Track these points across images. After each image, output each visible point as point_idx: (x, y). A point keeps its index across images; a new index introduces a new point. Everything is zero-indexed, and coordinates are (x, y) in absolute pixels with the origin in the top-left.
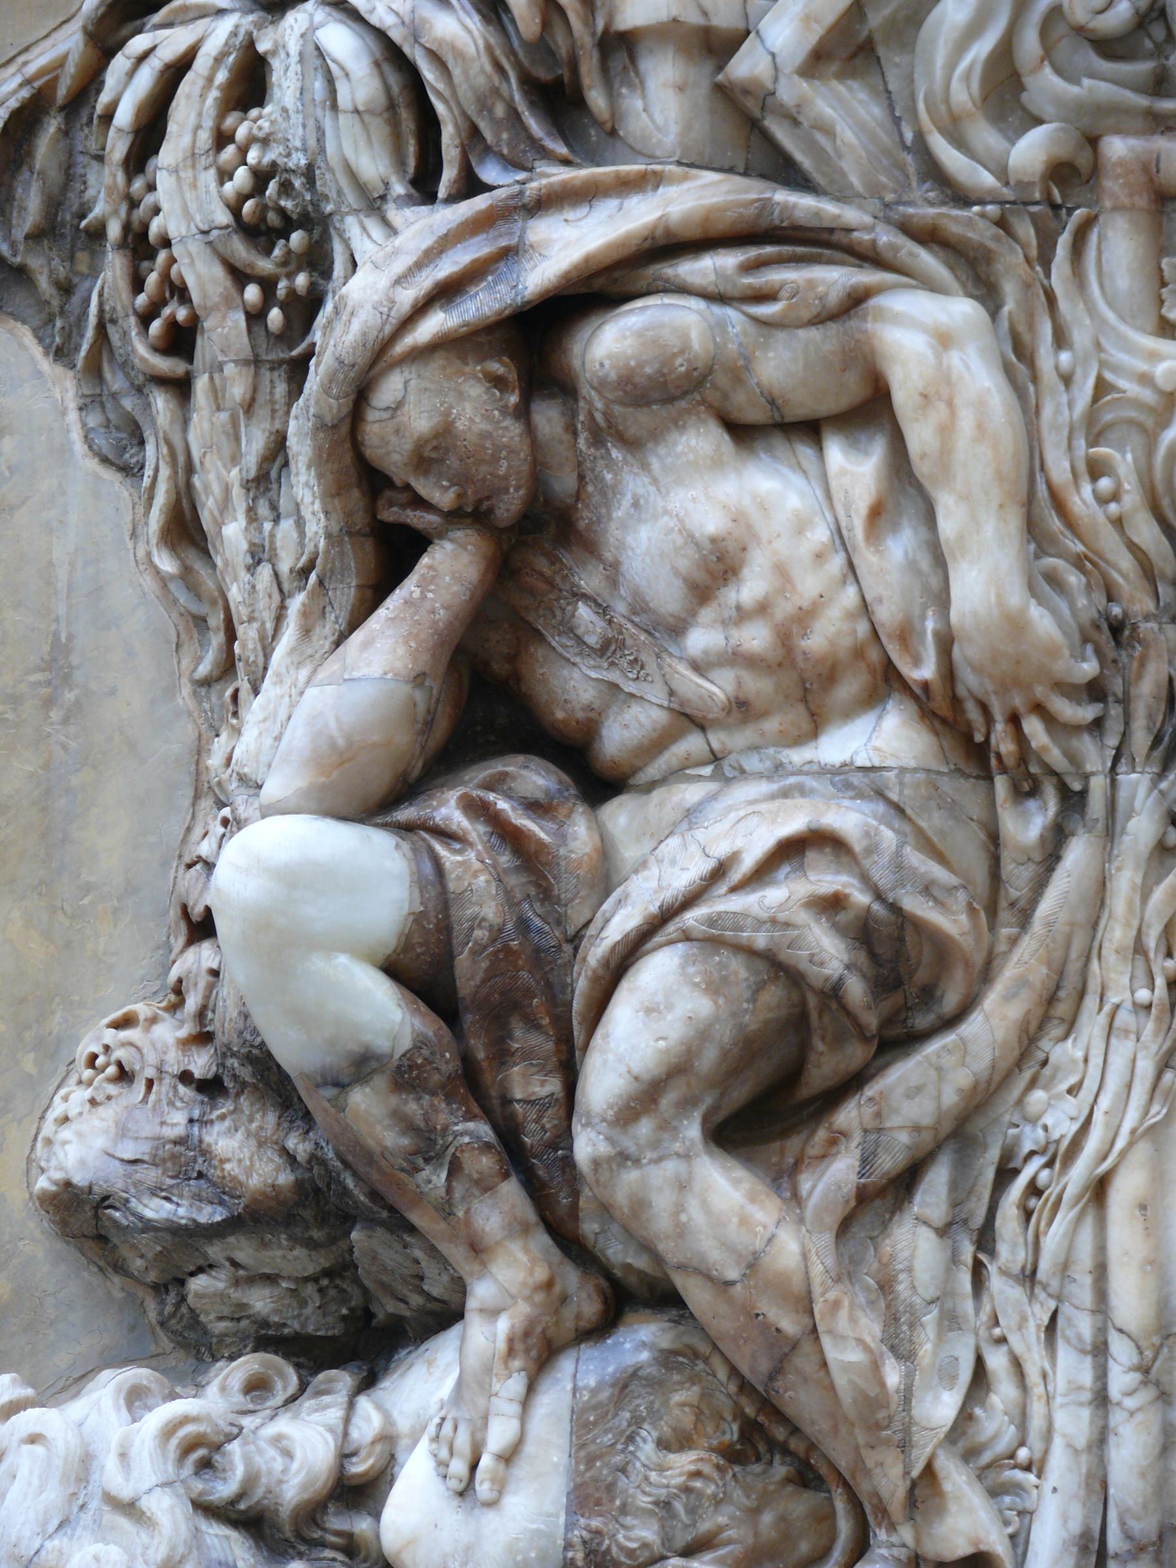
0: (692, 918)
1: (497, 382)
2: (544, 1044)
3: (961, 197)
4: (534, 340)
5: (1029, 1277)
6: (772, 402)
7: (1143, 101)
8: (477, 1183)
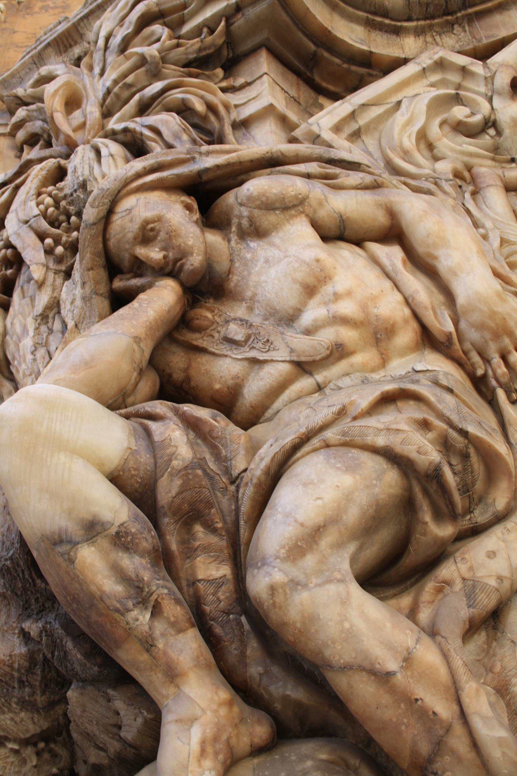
0: (330, 434)
1: (188, 207)
2: (219, 542)
3: (413, 177)
6: (341, 216)
7: (491, 155)
8: (173, 625)
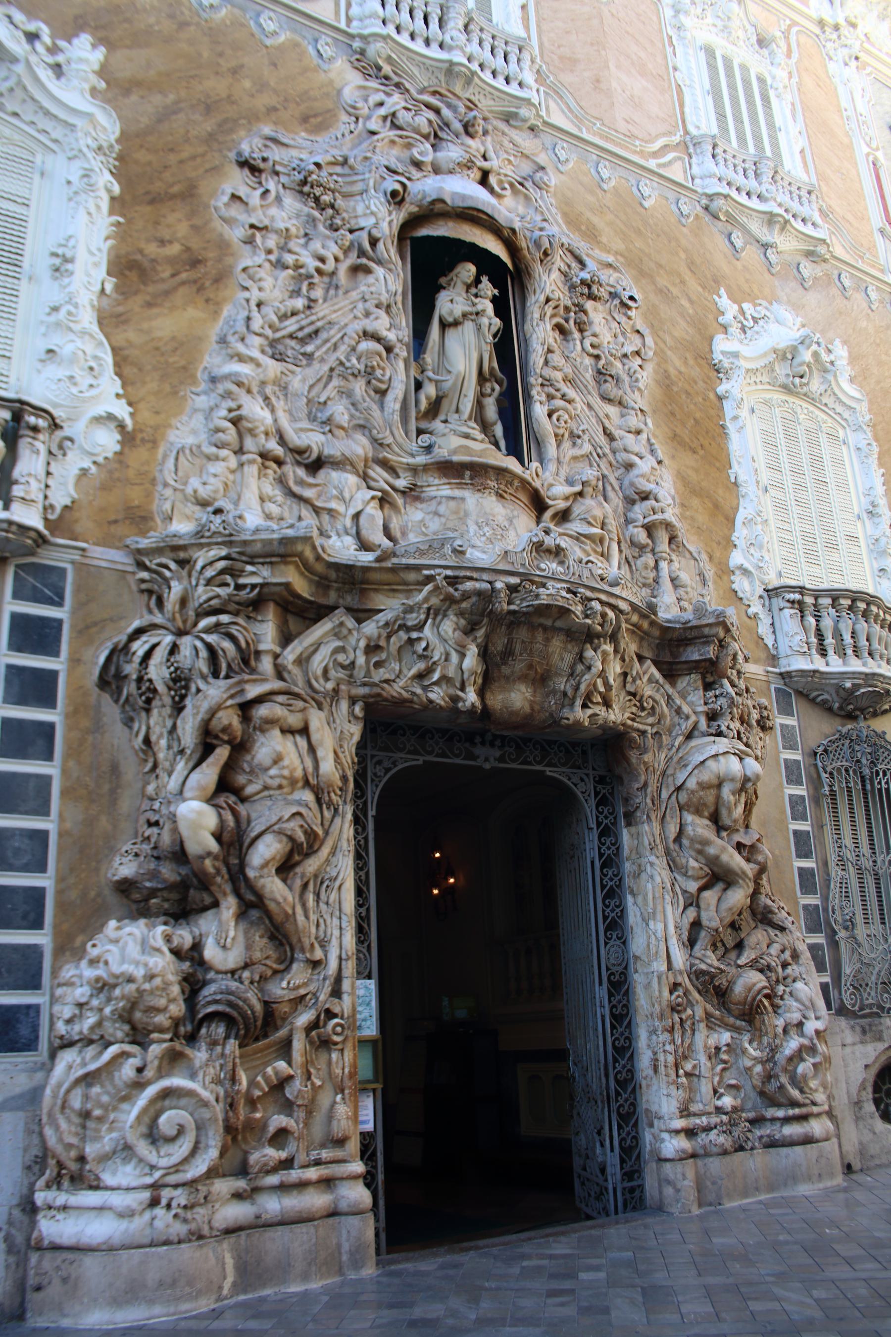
0: (276, 828)
4: (246, 708)
5: (327, 903)
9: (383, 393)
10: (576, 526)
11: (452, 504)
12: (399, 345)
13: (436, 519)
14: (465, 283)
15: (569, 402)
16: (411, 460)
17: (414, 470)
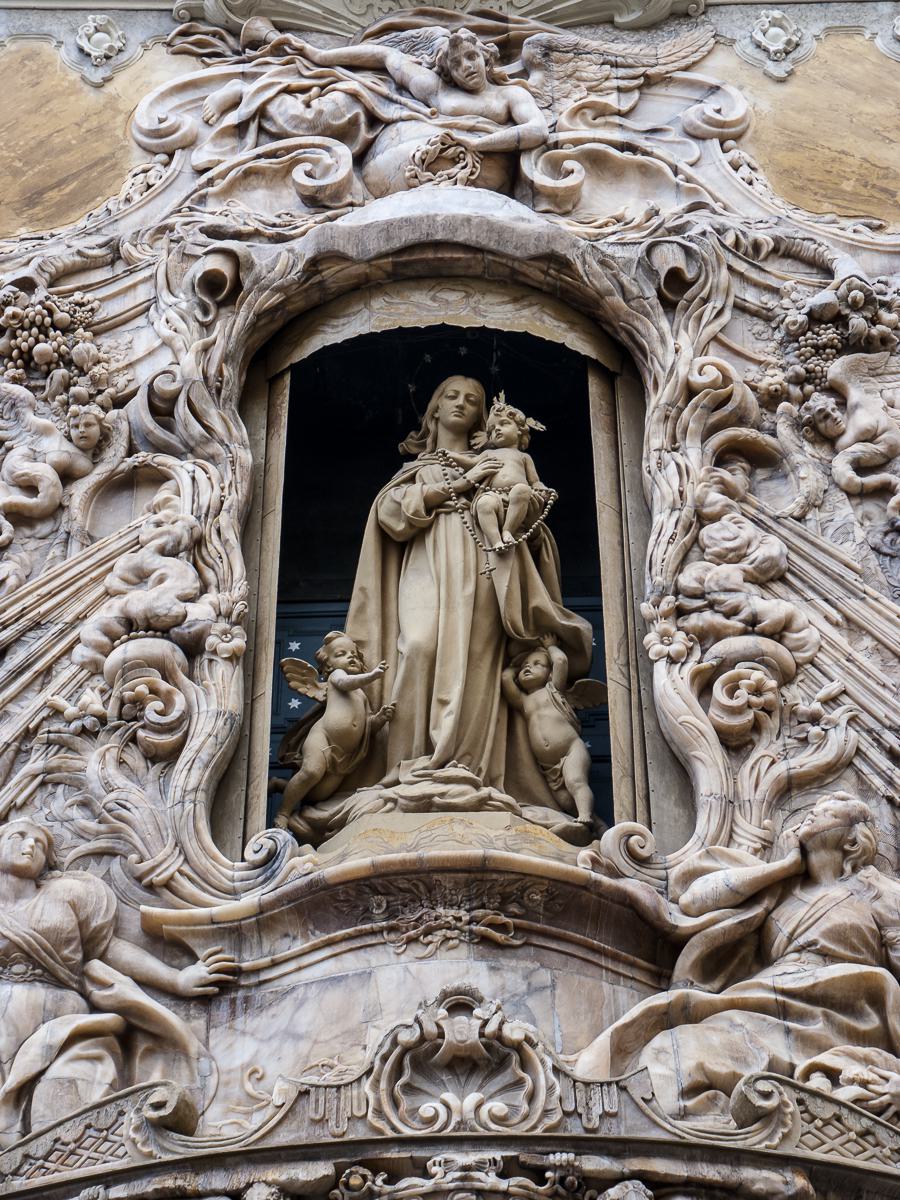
9: (165, 758)
10: (791, 973)
11: (334, 997)
12: (223, 625)
13: (289, 1049)
14: (453, 428)
15: (779, 632)
16: (224, 907)
17: (234, 932)
